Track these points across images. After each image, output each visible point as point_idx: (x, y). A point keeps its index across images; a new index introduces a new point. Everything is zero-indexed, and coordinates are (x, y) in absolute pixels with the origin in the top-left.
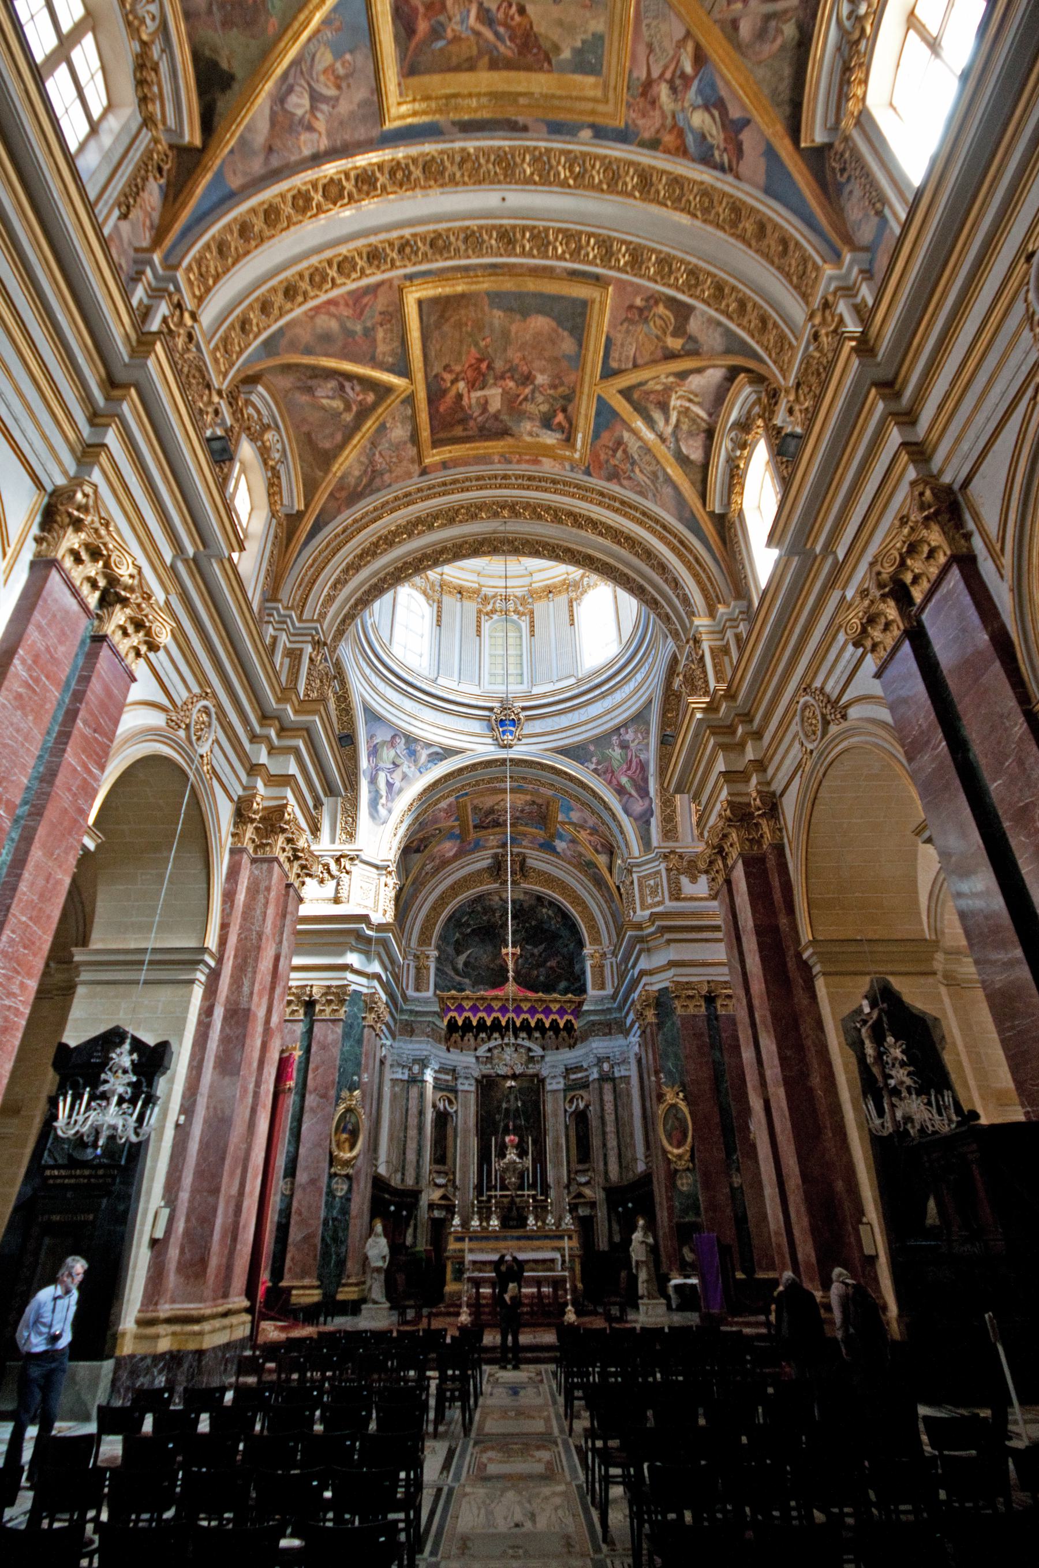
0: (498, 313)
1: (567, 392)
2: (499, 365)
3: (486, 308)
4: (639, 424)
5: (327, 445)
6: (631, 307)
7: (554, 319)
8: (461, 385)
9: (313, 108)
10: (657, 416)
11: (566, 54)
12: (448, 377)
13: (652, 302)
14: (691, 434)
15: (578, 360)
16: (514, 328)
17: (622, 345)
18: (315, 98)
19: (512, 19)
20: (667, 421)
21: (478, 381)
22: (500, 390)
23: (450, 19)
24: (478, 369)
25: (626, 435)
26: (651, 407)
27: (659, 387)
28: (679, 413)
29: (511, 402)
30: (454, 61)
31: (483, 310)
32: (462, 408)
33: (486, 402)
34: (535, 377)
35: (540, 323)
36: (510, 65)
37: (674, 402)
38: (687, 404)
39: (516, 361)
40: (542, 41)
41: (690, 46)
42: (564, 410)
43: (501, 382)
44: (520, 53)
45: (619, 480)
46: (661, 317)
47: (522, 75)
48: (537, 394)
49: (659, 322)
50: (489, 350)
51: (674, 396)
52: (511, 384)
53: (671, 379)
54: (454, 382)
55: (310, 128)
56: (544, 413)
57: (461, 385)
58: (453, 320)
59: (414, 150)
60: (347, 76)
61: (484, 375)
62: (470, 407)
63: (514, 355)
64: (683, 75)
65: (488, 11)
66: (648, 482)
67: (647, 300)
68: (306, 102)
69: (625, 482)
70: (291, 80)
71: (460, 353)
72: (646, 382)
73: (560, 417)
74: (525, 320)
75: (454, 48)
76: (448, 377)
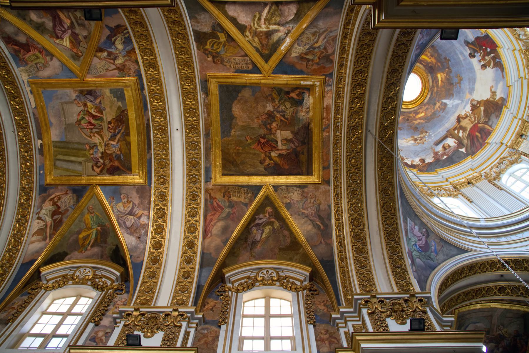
0: (233, 132)
1: (275, 92)
2: (262, 132)
3: (230, 138)
4: (283, 47)
5: (289, 240)
6: (214, 62)
7: (233, 102)
8: (273, 154)
10: (276, 37)
11: (120, 104)
12: (267, 161)
13: (207, 52)
14: (281, 15)
15: (255, 88)
16: (240, 124)
17: (237, 64)
18: (130, 213)
19: (113, 126)
20: (277, 31)
21: (272, 145)
22: (278, 131)
23: (114, 152)
24: (264, 144)
25: (294, 55)
26: (271, 42)
27: (256, 39)
28: (269, 24)
29: (285, 125)
30: (127, 151)
31: (231, 141)
32: (288, 154)
33: (286, 139)
34: (268, 111)
35: (236, 109)
36: (128, 128)
37: (264, 28)
38: (263, 20)
39: (260, 122)
40: (118, 114)
42: (288, 93)
43: (273, 130)
44: (123, 123)
45: (329, 55)
46: (212, 46)
47: (130, 122)
48: (280, 109)
49: (215, 47)
50: (253, 137)
51: (260, 29)
52: (274, 124)
53: (248, 33)
54: (270, 158)
55: (139, 218)
56: (291, 104)
57: (273, 154)
58: (235, 157)
60: (128, 197)
61: (268, 141)
62: (288, 150)
63: (256, 123)
65: (111, 136)
66: (322, 37)
67: (207, 55)
68: (132, 217)
69: (330, 51)
71: (254, 154)
72: (255, 47)
73: (293, 95)
74: (236, 118)
75: (123, 151)
76: (267, 161)
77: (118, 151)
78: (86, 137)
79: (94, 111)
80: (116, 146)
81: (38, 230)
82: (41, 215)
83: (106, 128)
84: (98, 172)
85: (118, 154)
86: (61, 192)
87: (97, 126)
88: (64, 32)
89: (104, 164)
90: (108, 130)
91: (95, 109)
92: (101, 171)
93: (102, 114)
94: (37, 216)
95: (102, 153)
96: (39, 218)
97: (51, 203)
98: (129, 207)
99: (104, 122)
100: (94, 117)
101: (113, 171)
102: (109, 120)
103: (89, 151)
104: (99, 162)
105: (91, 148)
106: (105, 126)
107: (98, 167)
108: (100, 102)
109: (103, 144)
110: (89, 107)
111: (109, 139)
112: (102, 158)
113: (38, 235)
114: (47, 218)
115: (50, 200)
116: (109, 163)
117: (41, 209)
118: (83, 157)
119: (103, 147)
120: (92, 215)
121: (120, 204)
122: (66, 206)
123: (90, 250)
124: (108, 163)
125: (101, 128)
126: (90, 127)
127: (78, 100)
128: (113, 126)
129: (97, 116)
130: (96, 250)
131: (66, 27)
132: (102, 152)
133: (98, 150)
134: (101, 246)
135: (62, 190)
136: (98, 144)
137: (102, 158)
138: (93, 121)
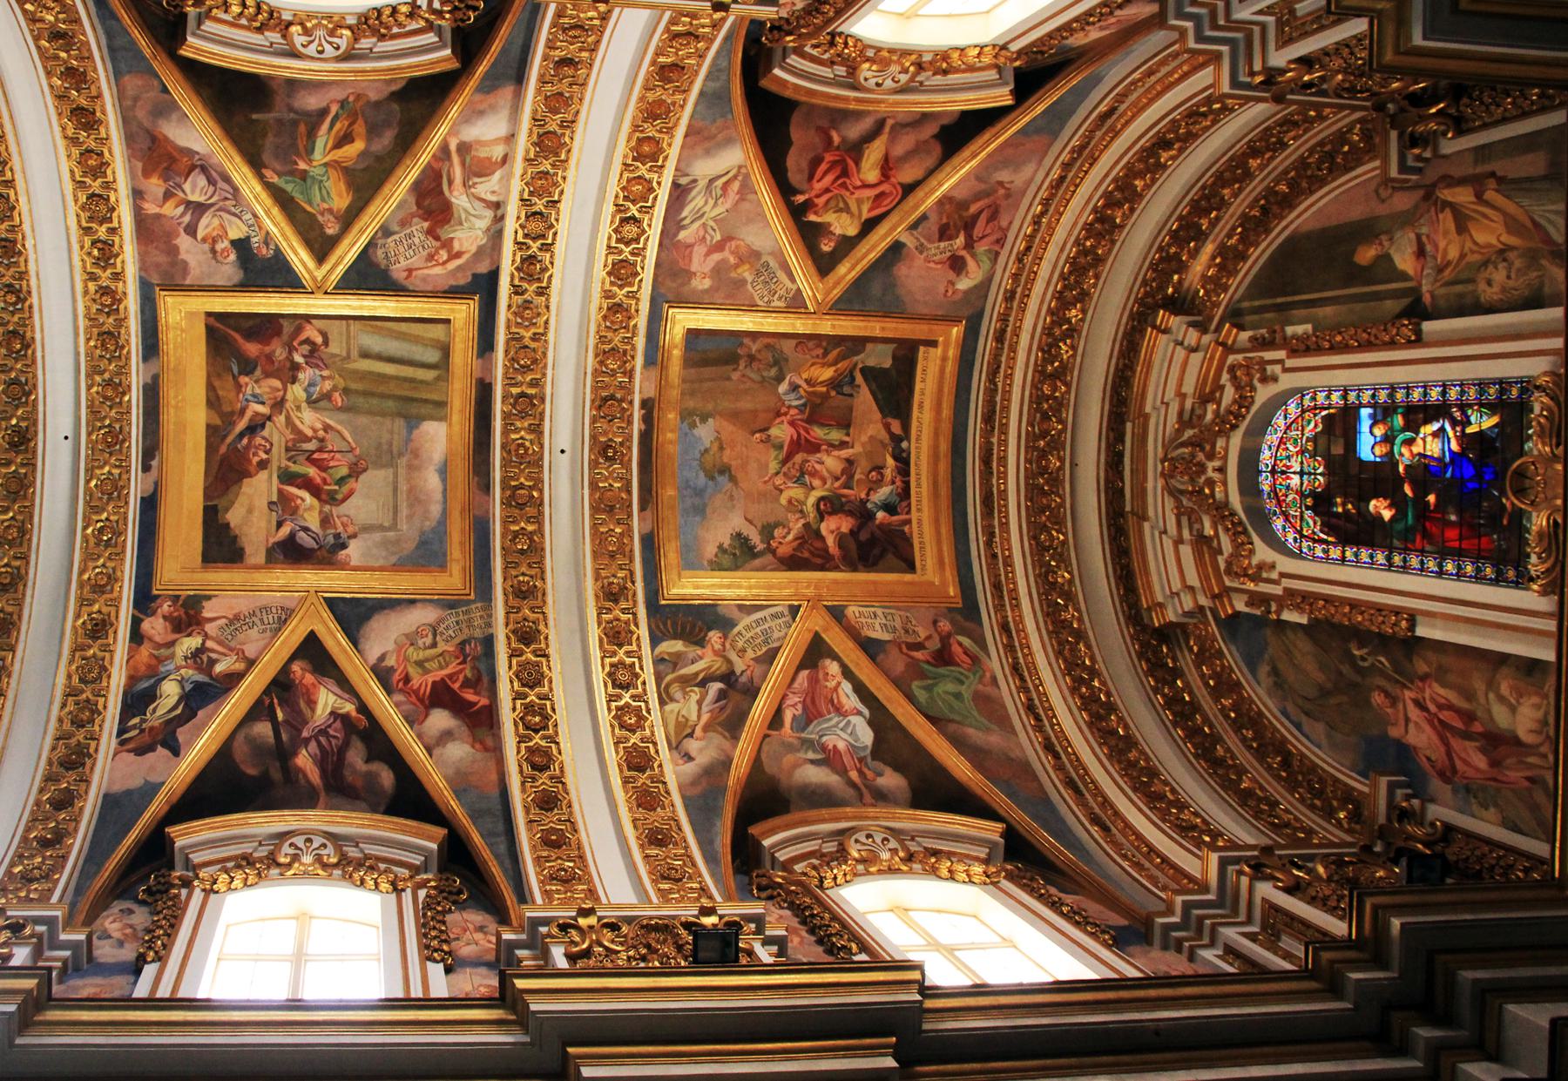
9: (188, 204)
18: (199, 209)
19: (255, 454)
23: (257, 382)
30: (217, 383)
36: (211, 449)
41: (240, 666)
55: (168, 195)
59: (134, 325)
60: (213, 251)
64: (213, 662)
65: (263, 426)
68: (195, 197)
70: (221, 184)
77: (247, 384)
78: (339, 427)
79: (303, 500)
80: (250, 398)
81: (493, 173)
82: (489, 214)
83: (275, 450)
84: (308, 327)
85: (247, 375)
86: (429, 275)
87: (302, 458)
88: (323, 732)
89: (291, 349)
90: (272, 445)
91: (297, 507)
92: (299, 330)
93: (280, 492)
94: (499, 213)
95: (294, 380)
96: (497, 205)
97: (456, 246)
98: (207, 227)
99: (279, 468)
100: (307, 484)
101: (265, 326)
102: (263, 475)
103: (335, 388)
104: (304, 356)
105: (327, 396)
106: (278, 458)
107: (308, 341)
108: (280, 525)
109: (289, 405)
110: (316, 514)
111: (269, 418)
112: (296, 367)
113: (489, 159)
114: (467, 205)
115: (458, 255)
116: (274, 351)
117: (488, 229)
118: (356, 372)
119: (289, 396)
120: (326, 206)
121: (235, 234)
122: (410, 236)
123: (331, 102)
124: (278, 352)
125: (292, 450)
126: (325, 456)
127: (344, 536)
128: (255, 454)
129: (299, 487)
130: (312, 102)
131: (313, 745)
132: (293, 383)
133: (306, 390)
134: (296, 112)
135: (424, 279)
136: (304, 405)
137: (296, 367)
138: (312, 471)
